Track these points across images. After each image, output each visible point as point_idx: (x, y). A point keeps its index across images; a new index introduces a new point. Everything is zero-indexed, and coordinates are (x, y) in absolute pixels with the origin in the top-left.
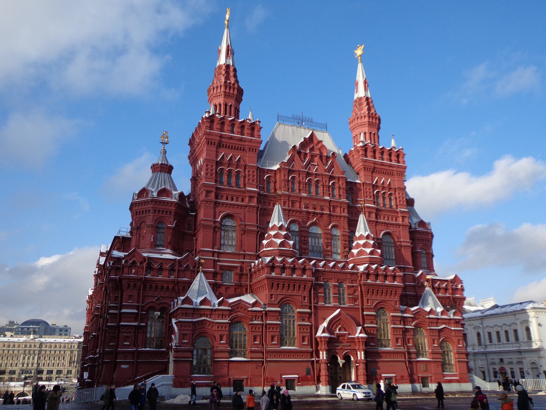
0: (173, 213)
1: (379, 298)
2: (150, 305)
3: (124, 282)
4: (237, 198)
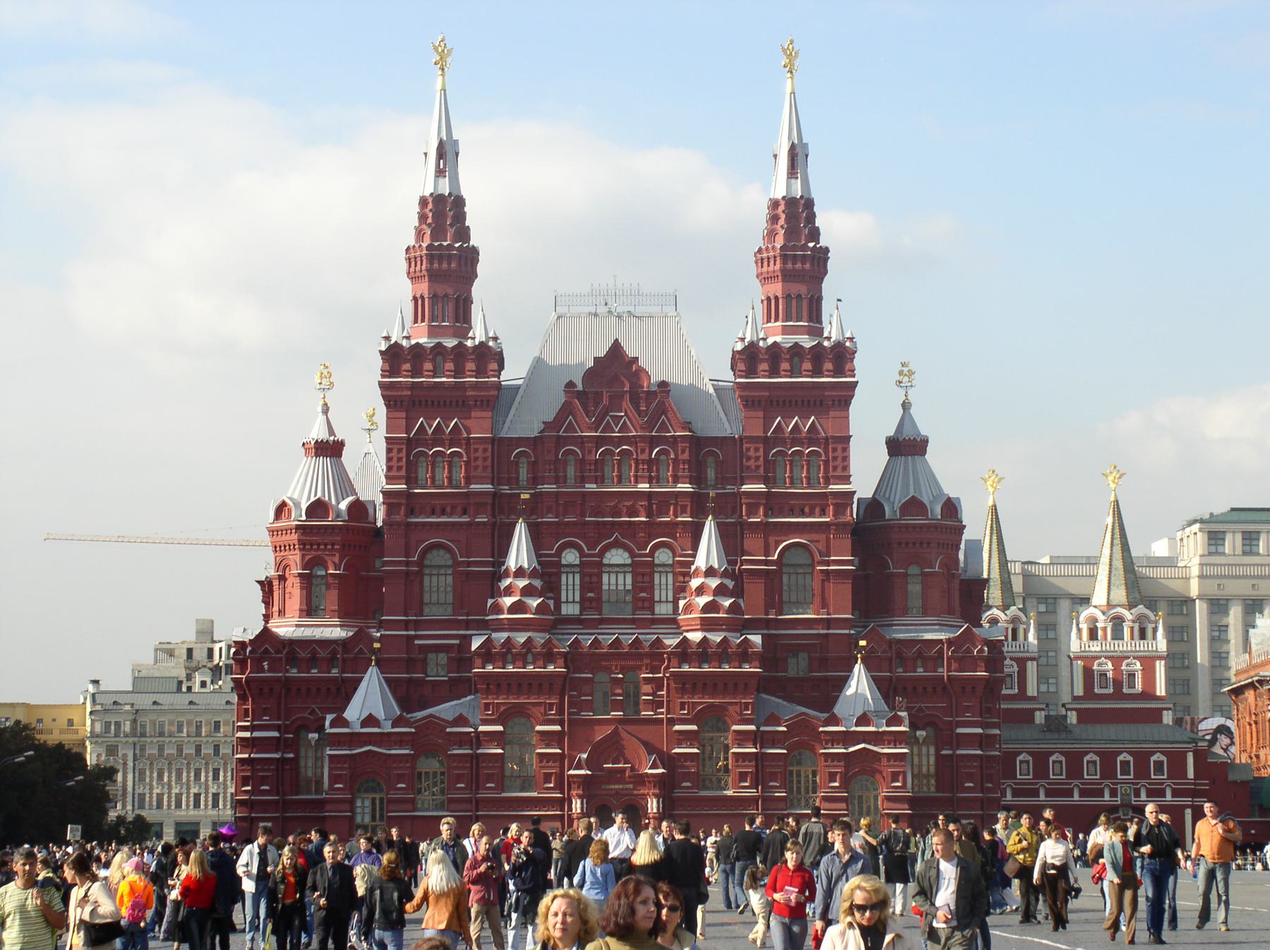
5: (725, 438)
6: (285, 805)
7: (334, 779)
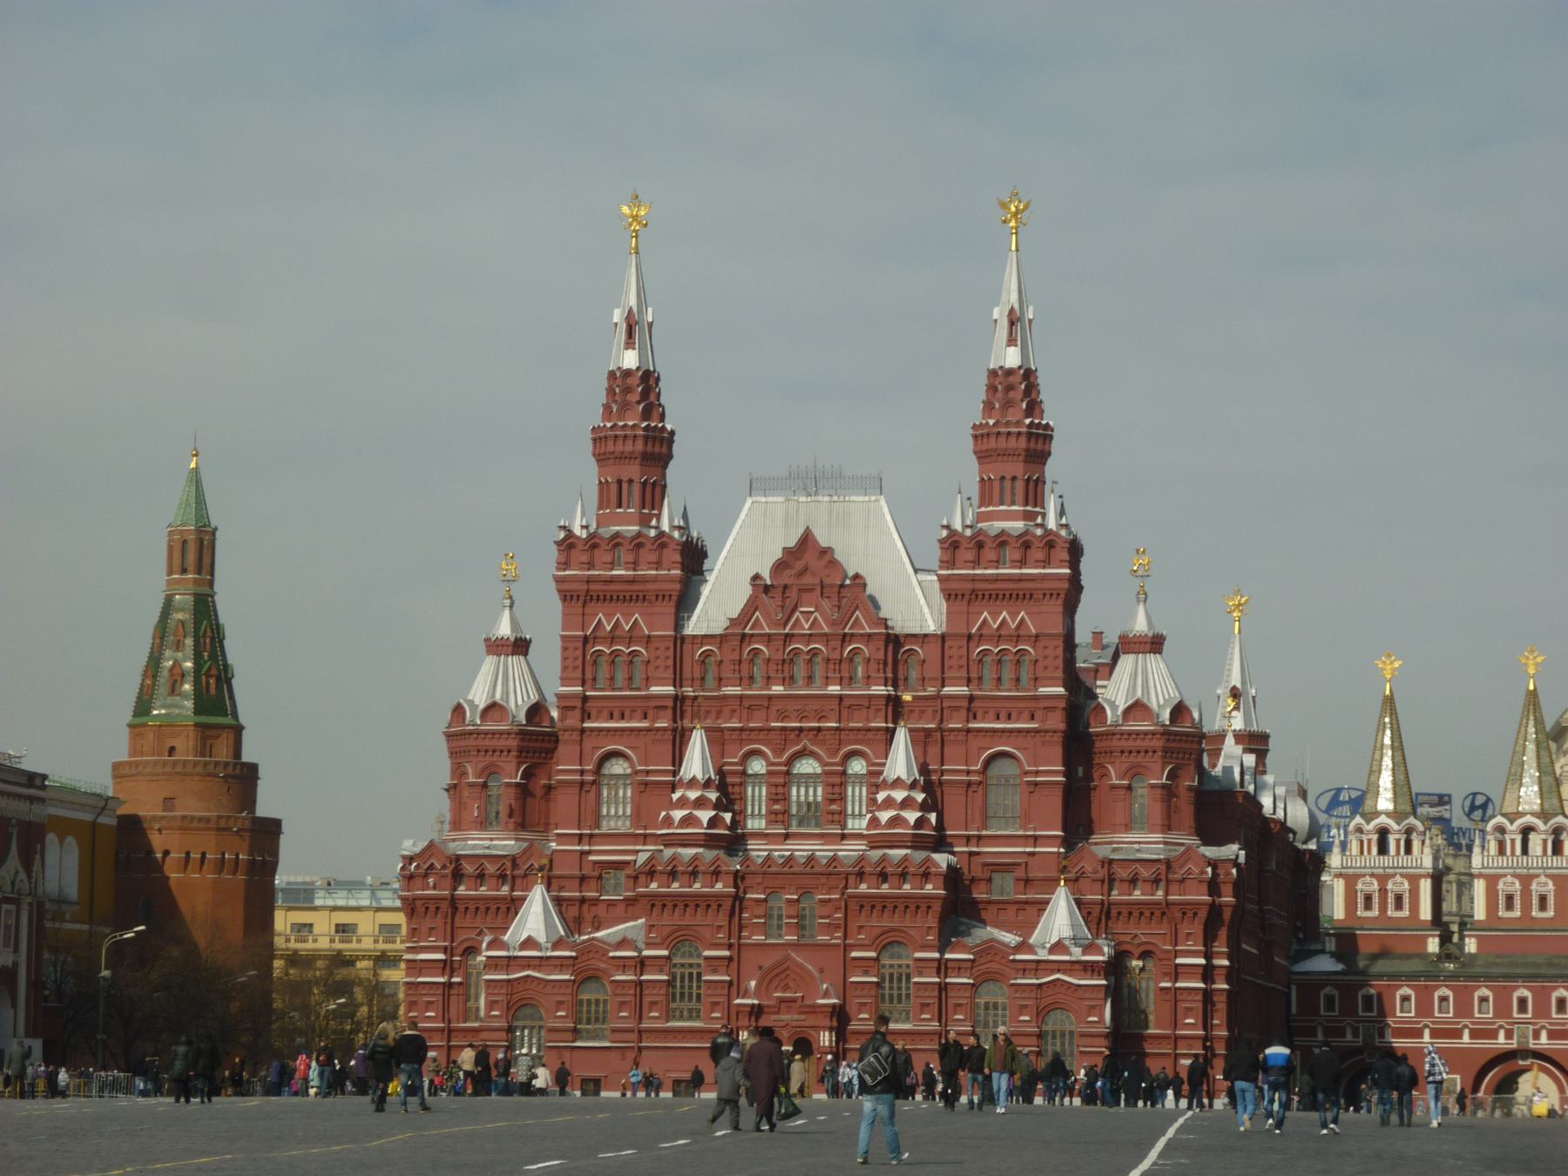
1: (887, 922)
2: (466, 945)
3: (419, 903)
4: (633, 711)
5: (926, 636)
6: (450, 1031)
7: (491, 1005)
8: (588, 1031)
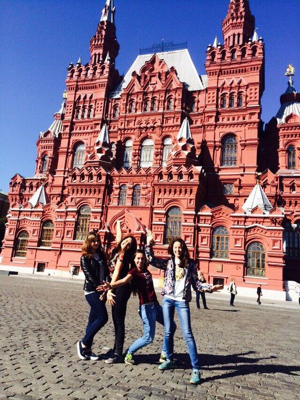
0: (52, 147)
1: (171, 196)
5: (200, 91)
8: (44, 242)
